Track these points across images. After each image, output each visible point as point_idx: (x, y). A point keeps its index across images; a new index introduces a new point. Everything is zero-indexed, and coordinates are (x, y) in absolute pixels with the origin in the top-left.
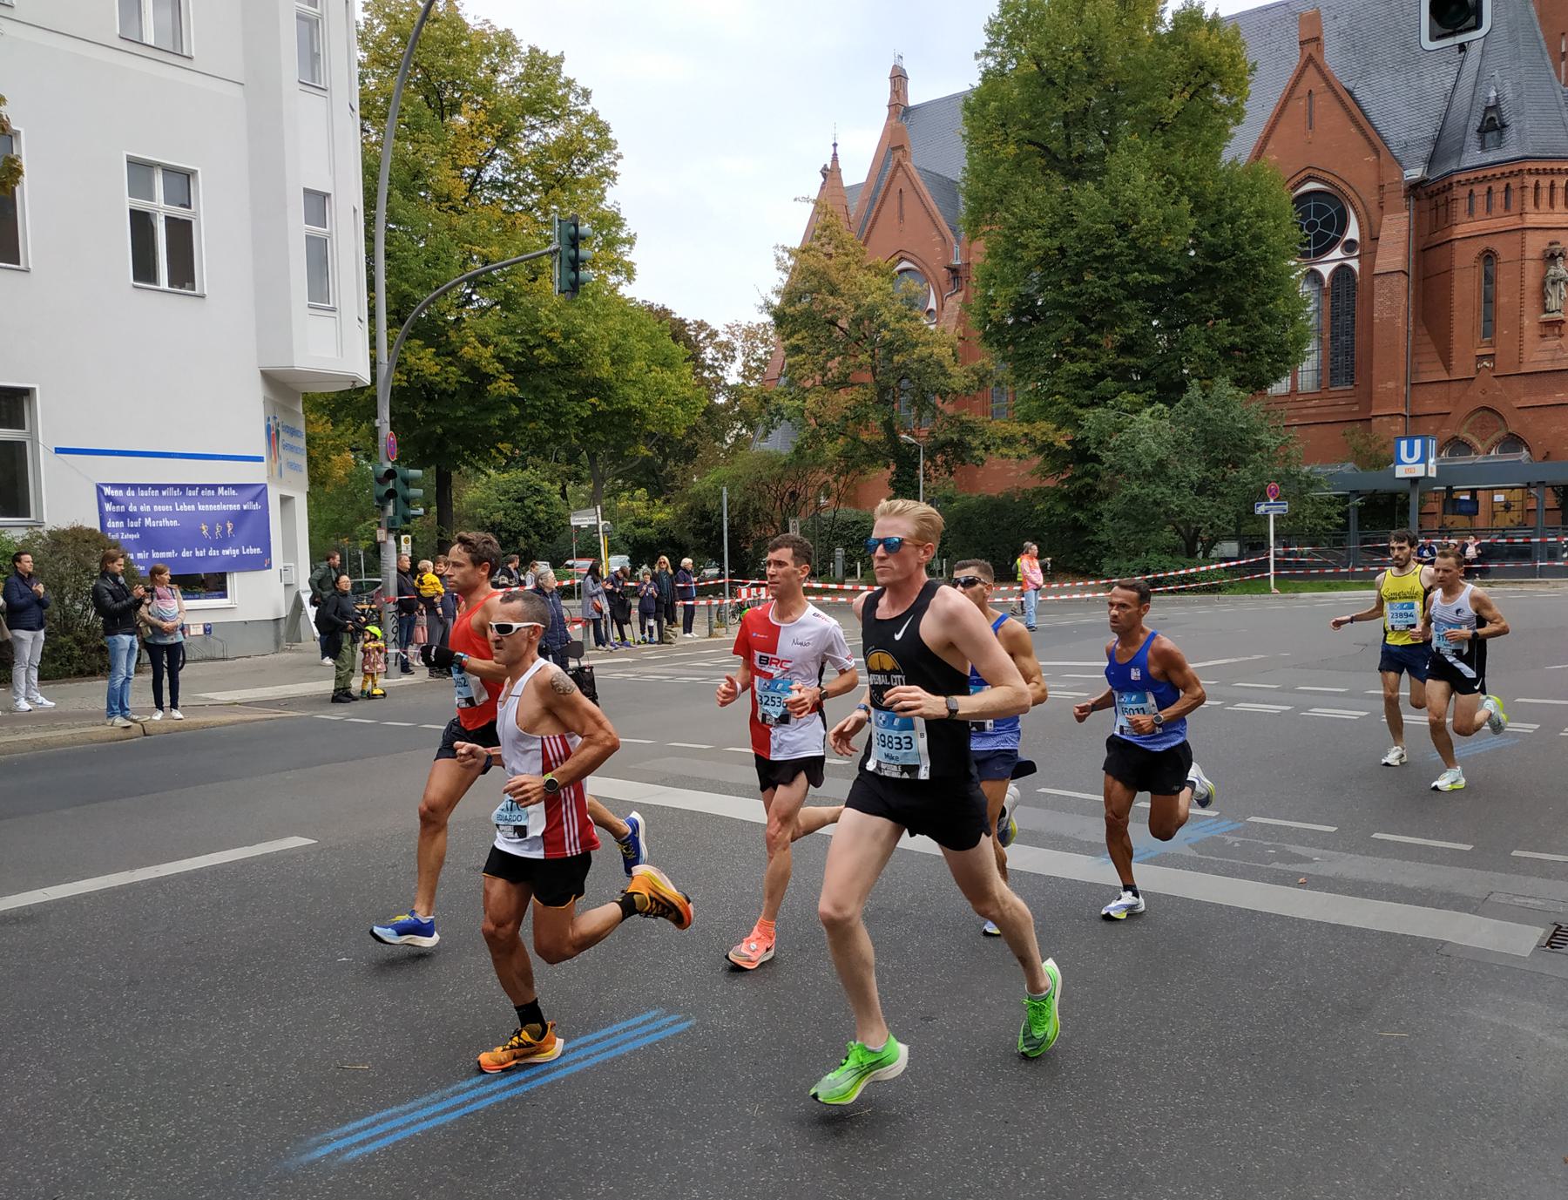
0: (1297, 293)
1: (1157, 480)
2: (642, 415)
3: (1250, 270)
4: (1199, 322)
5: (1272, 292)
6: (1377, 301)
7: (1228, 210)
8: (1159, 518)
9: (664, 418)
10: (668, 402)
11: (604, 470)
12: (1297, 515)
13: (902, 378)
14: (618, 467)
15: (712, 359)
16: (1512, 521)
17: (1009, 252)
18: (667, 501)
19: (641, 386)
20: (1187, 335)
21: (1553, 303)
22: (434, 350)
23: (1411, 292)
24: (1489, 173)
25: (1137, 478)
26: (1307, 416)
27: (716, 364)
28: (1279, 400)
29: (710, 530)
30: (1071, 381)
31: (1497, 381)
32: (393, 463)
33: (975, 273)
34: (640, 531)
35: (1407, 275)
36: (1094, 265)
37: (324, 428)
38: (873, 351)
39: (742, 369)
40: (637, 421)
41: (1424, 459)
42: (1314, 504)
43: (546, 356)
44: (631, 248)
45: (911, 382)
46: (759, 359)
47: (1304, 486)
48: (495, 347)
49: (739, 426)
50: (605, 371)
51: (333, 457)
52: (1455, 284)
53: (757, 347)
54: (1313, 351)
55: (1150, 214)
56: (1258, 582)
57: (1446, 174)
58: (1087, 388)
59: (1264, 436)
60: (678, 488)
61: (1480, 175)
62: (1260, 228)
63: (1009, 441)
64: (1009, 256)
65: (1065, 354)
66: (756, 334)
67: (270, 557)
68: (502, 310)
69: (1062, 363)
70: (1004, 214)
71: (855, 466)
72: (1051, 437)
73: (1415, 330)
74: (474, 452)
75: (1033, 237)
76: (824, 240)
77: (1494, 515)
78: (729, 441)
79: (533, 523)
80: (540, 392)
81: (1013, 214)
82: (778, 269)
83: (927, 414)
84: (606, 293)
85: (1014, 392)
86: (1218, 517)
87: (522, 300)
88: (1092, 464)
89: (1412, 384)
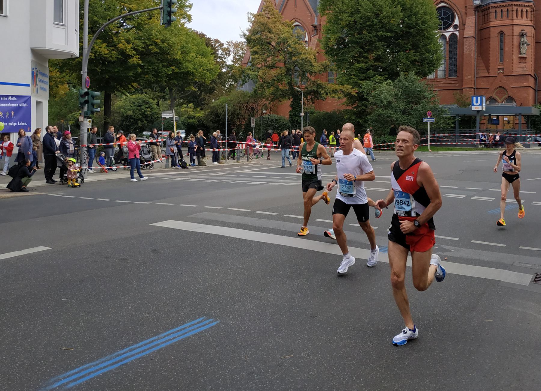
0: (438, 42)
1: (388, 108)
2: (193, 74)
3: (422, 33)
4: (403, 51)
5: (429, 41)
6: (465, 47)
7: (414, 11)
8: (389, 122)
9: (202, 76)
10: (204, 70)
11: (175, 95)
12: (438, 123)
13: (295, 66)
14: (182, 94)
15: (221, 54)
16: (510, 127)
17: (336, 21)
18: (201, 109)
19: (193, 63)
20: (399, 56)
21: (523, 51)
22: (106, 44)
23: (476, 44)
24: (502, 4)
25: (381, 107)
26: (440, 87)
27: (223, 56)
28: (431, 81)
29: (220, 120)
30: (358, 71)
31: (505, 78)
32: (88, 89)
33: (323, 28)
34: (190, 121)
35: (475, 38)
36: (367, 28)
37: (56, 74)
38: (285, 55)
39: (233, 59)
40: (191, 77)
41: (481, 104)
42: (443, 119)
43: (154, 49)
44: (190, 9)
45: (299, 67)
46: (240, 56)
47: (440, 112)
48: (133, 44)
49: (231, 81)
50: (179, 56)
51: (59, 86)
52: (491, 42)
53: (239, 51)
54: (443, 64)
55: (387, 11)
56: (425, 147)
57: (488, 4)
58: (363, 73)
59: (426, 94)
60: (207, 104)
61: (499, 5)
62: (425, 18)
63: (335, 92)
64: (336, 22)
65: (355, 60)
66: (238, 46)
67: (31, 126)
68: (136, 30)
69: (355, 64)
70: (334, 7)
71: (277, 98)
72: (350, 91)
73: (477, 58)
74: (121, 86)
75: (345, 16)
76: (266, 12)
77: (504, 125)
78: (227, 86)
79: (145, 116)
80: (150, 63)
81: (338, 7)
82: (249, 21)
83: (305, 80)
84: (180, 26)
85: (337, 74)
86: (410, 123)
87: (145, 26)
88: (365, 102)
89: (477, 77)
